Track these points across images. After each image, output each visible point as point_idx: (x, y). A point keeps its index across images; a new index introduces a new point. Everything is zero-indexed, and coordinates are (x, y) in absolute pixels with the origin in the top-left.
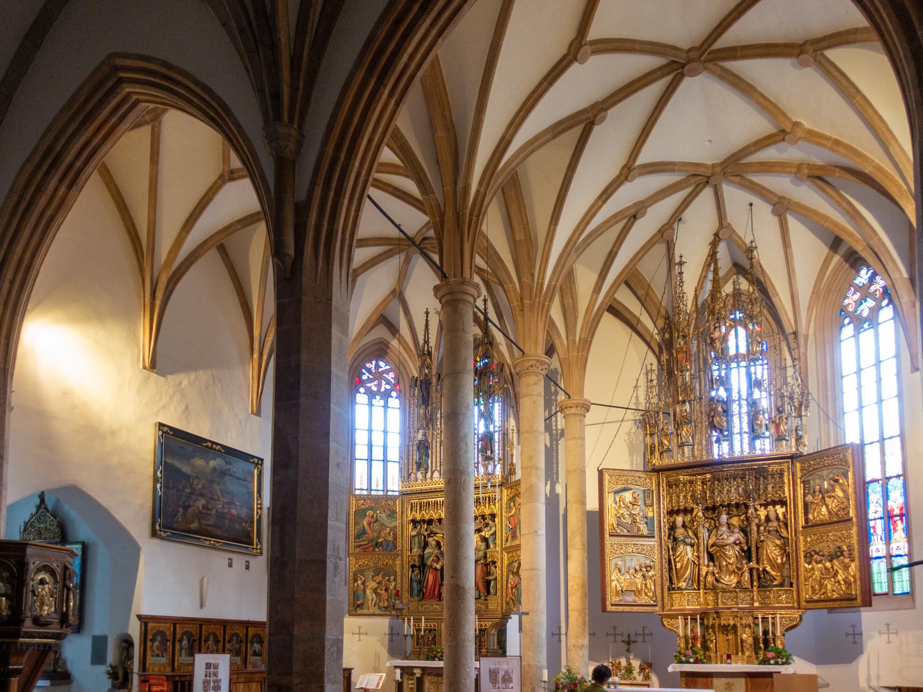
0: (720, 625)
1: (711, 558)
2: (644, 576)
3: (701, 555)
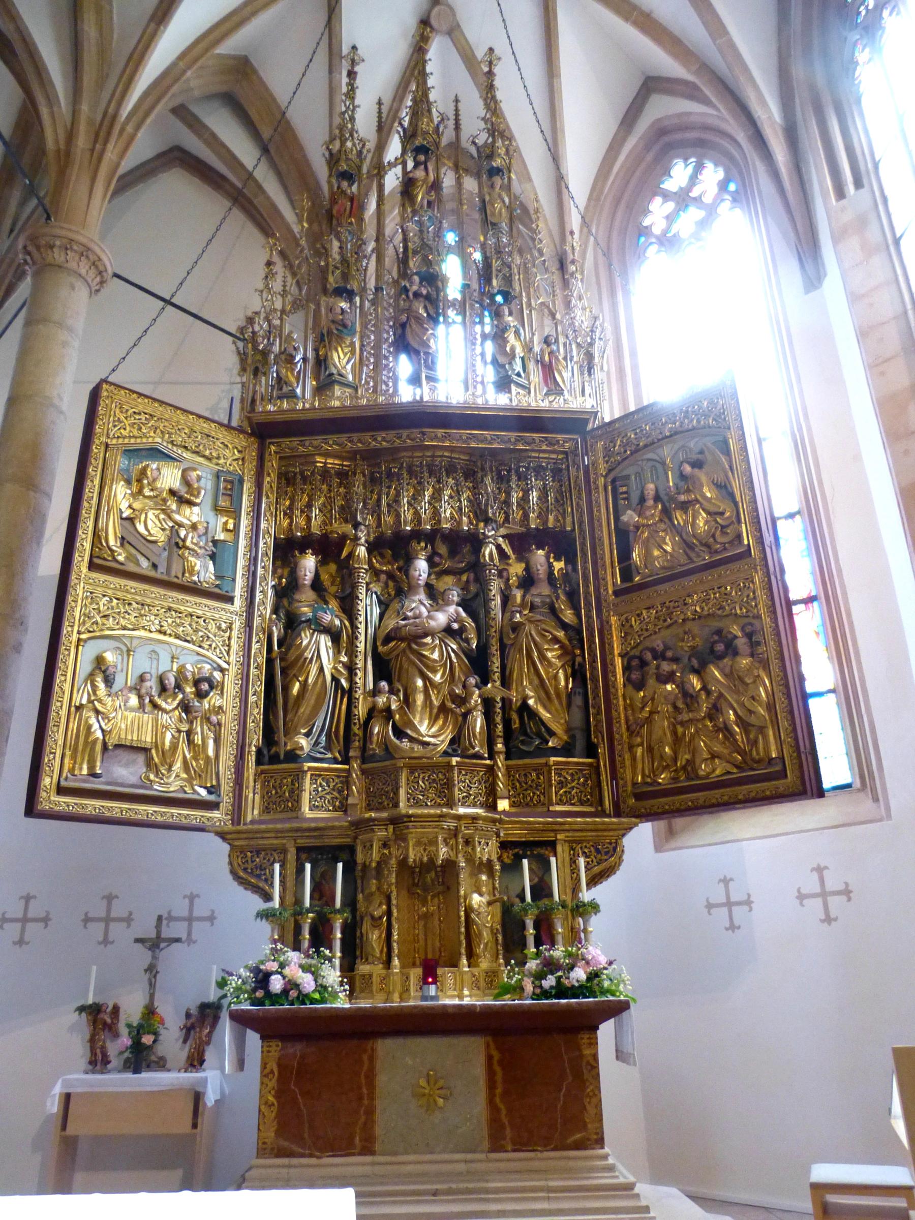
0: (403, 863)
1: (383, 669)
2: (186, 707)
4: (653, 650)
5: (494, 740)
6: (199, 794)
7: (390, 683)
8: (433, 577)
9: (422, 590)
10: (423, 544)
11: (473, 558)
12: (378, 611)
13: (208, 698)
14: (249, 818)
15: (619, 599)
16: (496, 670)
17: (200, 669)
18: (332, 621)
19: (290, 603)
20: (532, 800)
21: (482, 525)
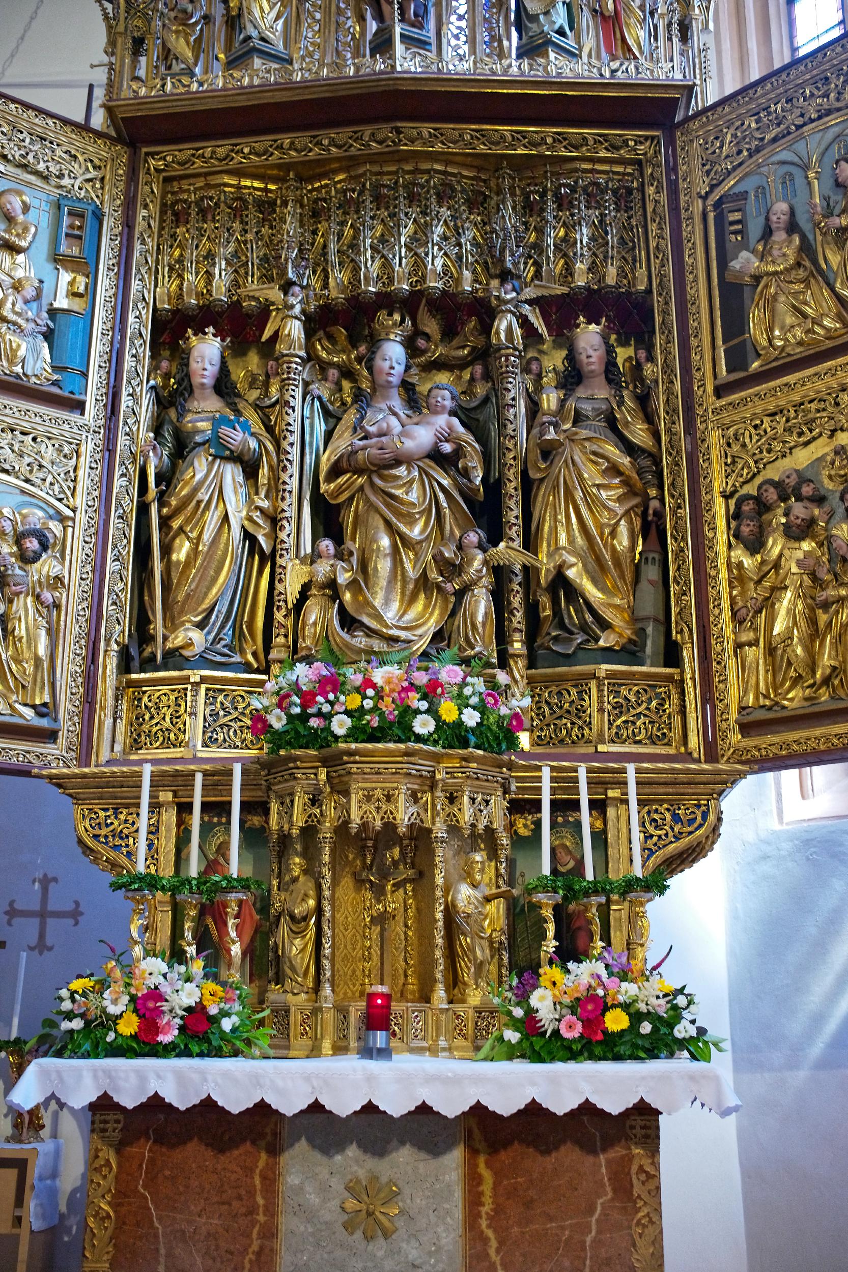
1: (328, 520)
3: (289, 506)
4: (777, 485)
5: (510, 636)
6: (21, 716)
7: (339, 541)
8: (414, 371)
9: (394, 392)
10: (397, 317)
11: (481, 342)
12: (323, 427)
13: (37, 565)
14: (105, 755)
15: (723, 402)
16: (513, 521)
17: (24, 517)
18: (245, 441)
19: (181, 416)
20: (569, 734)
21: (495, 283)
